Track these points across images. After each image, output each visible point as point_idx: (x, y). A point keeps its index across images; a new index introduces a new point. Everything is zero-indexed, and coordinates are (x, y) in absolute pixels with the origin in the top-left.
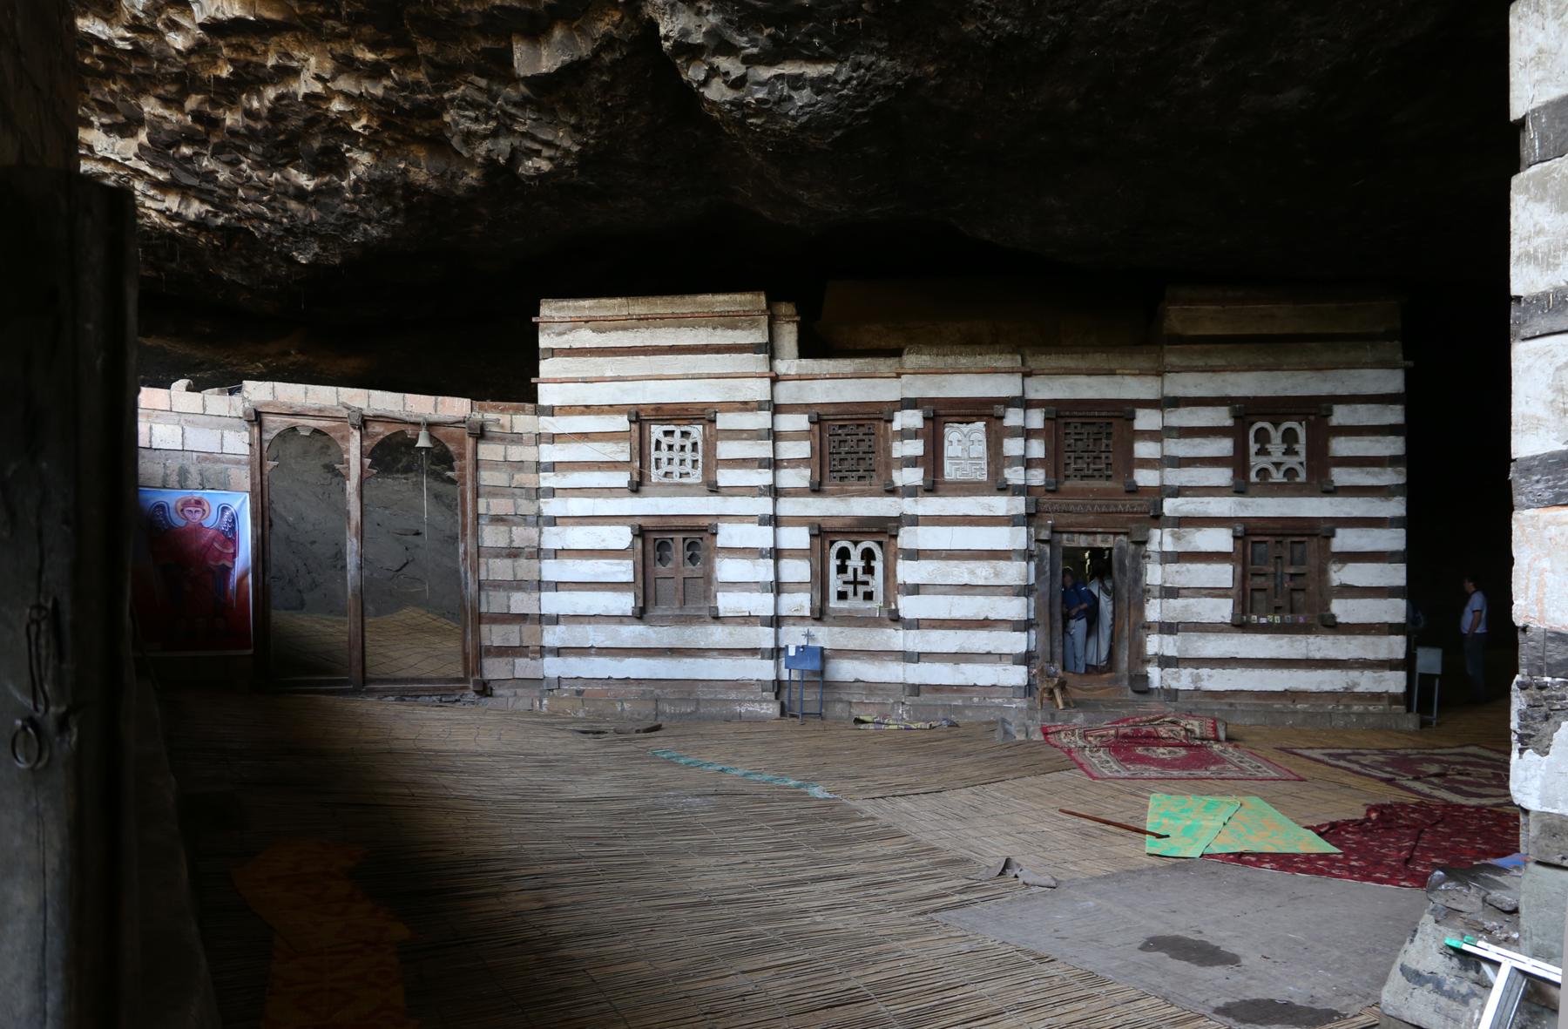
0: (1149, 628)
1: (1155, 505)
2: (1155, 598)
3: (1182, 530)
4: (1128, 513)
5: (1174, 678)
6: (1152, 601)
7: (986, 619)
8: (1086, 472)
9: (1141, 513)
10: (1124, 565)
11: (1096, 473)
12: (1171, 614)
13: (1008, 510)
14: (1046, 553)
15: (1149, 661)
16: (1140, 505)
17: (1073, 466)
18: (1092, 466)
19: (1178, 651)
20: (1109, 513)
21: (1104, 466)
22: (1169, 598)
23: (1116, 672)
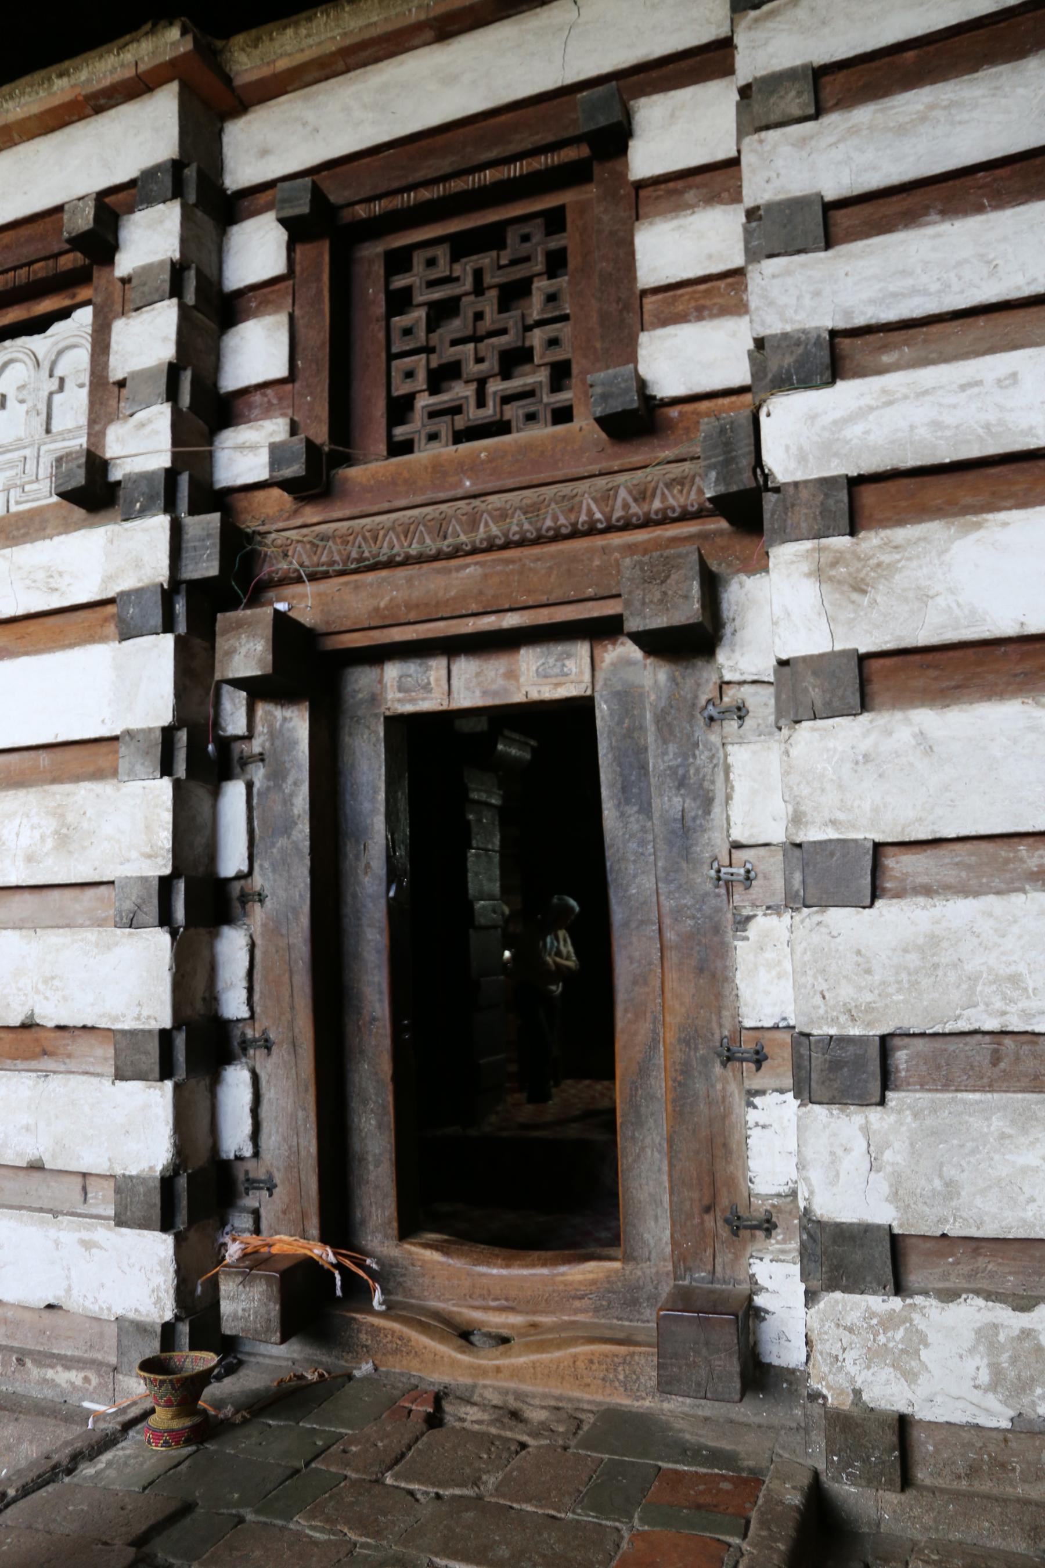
3: (871, 540)
4: (627, 526)
7: (28, 1026)
8: (474, 415)
9: (685, 516)
11: (513, 412)
12: (846, 993)
13: (108, 579)
14: (295, 743)
17: (424, 401)
18: (495, 387)
21: (542, 376)
23: (627, 1258)
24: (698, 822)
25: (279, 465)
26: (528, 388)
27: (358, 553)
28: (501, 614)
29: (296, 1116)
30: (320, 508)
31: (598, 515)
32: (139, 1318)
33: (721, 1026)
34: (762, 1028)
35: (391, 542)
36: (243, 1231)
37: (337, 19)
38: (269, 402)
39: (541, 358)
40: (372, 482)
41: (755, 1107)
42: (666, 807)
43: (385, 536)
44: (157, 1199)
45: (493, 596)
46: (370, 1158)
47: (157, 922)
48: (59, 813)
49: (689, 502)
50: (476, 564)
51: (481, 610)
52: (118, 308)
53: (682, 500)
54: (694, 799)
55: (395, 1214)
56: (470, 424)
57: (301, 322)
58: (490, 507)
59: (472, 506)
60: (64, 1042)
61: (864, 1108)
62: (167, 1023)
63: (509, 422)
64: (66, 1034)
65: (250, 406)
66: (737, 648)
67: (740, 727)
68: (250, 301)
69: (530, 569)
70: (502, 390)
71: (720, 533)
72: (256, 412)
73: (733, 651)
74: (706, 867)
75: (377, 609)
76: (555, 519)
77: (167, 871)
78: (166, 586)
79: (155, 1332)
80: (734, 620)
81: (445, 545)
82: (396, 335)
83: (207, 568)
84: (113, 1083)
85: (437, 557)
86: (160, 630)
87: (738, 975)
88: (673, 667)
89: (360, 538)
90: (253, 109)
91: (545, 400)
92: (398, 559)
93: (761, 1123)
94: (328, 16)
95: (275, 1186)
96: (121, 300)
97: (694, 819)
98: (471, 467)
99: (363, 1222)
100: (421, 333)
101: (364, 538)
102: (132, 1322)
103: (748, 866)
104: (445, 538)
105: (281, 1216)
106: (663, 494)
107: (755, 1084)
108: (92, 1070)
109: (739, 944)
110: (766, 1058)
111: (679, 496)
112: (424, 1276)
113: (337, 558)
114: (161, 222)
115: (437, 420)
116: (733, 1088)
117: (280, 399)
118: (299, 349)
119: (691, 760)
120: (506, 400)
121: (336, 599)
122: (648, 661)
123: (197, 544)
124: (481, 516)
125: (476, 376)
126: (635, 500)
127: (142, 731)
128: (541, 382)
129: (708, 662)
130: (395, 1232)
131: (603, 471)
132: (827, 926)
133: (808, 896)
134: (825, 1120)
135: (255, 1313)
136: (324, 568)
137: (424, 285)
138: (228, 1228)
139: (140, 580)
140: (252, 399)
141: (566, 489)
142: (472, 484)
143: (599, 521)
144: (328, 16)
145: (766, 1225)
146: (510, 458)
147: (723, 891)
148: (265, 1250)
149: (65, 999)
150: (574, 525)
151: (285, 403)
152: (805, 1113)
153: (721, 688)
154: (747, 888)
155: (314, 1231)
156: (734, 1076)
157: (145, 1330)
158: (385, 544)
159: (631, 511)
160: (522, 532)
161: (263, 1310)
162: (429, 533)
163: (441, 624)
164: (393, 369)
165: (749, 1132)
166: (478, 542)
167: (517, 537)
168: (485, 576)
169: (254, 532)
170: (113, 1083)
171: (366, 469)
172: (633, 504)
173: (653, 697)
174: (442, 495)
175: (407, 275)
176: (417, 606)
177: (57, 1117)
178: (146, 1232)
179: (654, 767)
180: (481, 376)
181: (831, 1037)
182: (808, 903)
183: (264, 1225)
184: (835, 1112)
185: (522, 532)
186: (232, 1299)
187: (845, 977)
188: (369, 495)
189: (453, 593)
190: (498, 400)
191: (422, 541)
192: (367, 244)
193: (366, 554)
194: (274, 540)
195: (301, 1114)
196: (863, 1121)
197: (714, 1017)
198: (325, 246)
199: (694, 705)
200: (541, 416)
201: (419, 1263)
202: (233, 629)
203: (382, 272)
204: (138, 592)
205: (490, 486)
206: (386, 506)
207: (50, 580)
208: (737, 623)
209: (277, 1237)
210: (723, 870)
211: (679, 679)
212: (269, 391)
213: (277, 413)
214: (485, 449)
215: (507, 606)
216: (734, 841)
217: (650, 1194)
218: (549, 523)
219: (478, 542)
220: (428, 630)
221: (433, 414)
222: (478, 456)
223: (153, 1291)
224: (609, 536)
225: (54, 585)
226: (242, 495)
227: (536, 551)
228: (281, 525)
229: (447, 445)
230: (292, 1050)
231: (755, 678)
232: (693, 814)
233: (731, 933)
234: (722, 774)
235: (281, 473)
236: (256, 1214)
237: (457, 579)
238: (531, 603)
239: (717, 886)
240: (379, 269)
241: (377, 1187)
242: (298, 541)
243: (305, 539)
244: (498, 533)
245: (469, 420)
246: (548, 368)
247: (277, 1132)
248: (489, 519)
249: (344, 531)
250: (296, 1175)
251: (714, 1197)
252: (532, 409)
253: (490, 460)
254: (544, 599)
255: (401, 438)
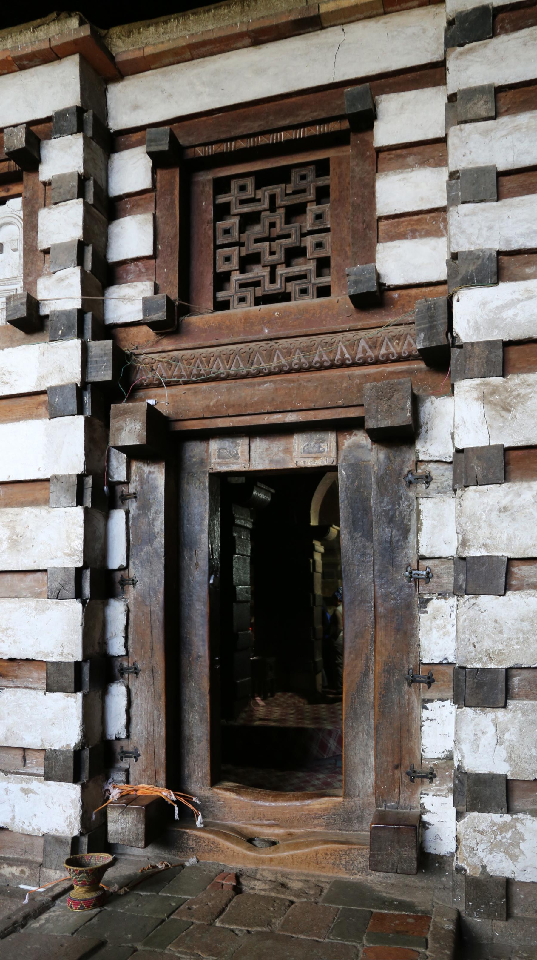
0: (430, 681)
1: (432, 318)
2: (443, 595)
4: (364, 363)
5: (494, 847)
6: (436, 604)
9: (400, 359)
10: (367, 510)
13: (41, 378)
15: (431, 776)
16: (398, 338)
17: (236, 277)
19: (509, 759)
20: (310, 369)
22: (477, 594)
24: (400, 543)
25: (149, 312)
26: (302, 273)
27: (197, 370)
28: (285, 414)
29: (153, 714)
30: (172, 341)
31: (347, 356)
32: (57, 834)
33: (408, 662)
34: (433, 664)
35: (218, 365)
36: (119, 782)
37: (185, 24)
38: (140, 270)
39: (311, 254)
40: (206, 326)
41: (427, 709)
42: (382, 534)
43: (214, 361)
44: (71, 764)
45: (281, 402)
46: (195, 739)
47: (74, 596)
48: (11, 526)
49: (403, 351)
50: (271, 381)
51: (273, 410)
52: (41, 201)
53: (399, 349)
54: (398, 530)
55: (209, 771)
56: (265, 293)
57: (160, 220)
58: (280, 346)
59: (269, 345)
60: (14, 669)
61: (495, 709)
62: (79, 658)
63: (290, 294)
64: (14, 664)
65: (127, 272)
66: (428, 441)
67: (427, 488)
68: (126, 204)
69: (304, 387)
70: (286, 273)
71: (419, 370)
72: (131, 276)
73: (426, 442)
74: (404, 570)
75: (208, 407)
76: (321, 356)
77: (80, 564)
78: (79, 385)
79: (68, 842)
80: (427, 423)
81: (253, 369)
82: (219, 233)
83: (104, 375)
84: (45, 694)
85: (247, 376)
86: (76, 413)
87: (421, 633)
88: (389, 450)
89: (198, 361)
90: (128, 77)
91: (313, 281)
92: (222, 376)
93: (430, 718)
94: (178, 21)
95: (139, 755)
96: (43, 196)
97: (398, 541)
98: (269, 321)
99: (189, 776)
100: (236, 233)
101: (201, 362)
102: (53, 837)
103: (428, 570)
104: (252, 364)
105: (142, 773)
106: (387, 345)
107: (427, 696)
108: (30, 685)
109: (422, 615)
110: (434, 681)
111: (396, 346)
112: (225, 807)
113: (184, 373)
114: (70, 147)
115: (245, 289)
116: (414, 698)
117: (147, 269)
118: (160, 237)
119: (397, 507)
120: (289, 279)
121: (182, 398)
122: (374, 446)
123: (98, 359)
124: (275, 352)
125: (270, 263)
126: (370, 348)
127: (65, 476)
128: (310, 270)
129: (410, 448)
130: (209, 782)
131: (351, 329)
132: (478, 606)
133: (468, 588)
134: (472, 716)
135: (130, 830)
136: (176, 379)
137: (238, 202)
138: (110, 781)
139: (62, 380)
140: (129, 267)
141: (328, 338)
142: (269, 332)
143: (348, 359)
144: (178, 21)
145: (430, 776)
146: (293, 316)
147: (413, 584)
148: (134, 793)
149: (15, 642)
150: (332, 361)
151: (150, 272)
152: (461, 712)
153: (416, 464)
154: (427, 583)
155: (163, 782)
156: (415, 691)
157: (61, 842)
158: (215, 366)
159: (367, 354)
160: (300, 363)
161: (134, 829)
162: (242, 361)
163: (248, 418)
164: (217, 255)
165: (423, 723)
166: (272, 368)
167: (296, 367)
168: (276, 390)
169: (132, 353)
170: (45, 694)
171: (203, 318)
172: (369, 350)
173: (376, 468)
174: (251, 338)
175: (227, 195)
176: (234, 406)
177: (9, 714)
178: (63, 783)
179: (375, 510)
180: (273, 263)
181: (478, 669)
182: (469, 592)
183: (132, 778)
184: (478, 712)
185: (300, 363)
186: (115, 822)
187: (487, 635)
188: (204, 335)
189: (256, 399)
190: (283, 279)
191: (238, 366)
192: (202, 173)
193: (202, 372)
194: (143, 360)
195: (156, 713)
196: (494, 717)
197: (405, 657)
198: (176, 172)
199: (400, 474)
200: (310, 291)
201: (223, 800)
202: (121, 415)
203: (211, 192)
204: (62, 388)
205: (281, 334)
206: (215, 342)
207: (3, 376)
208: (429, 426)
209: (141, 785)
210: (414, 572)
211: (392, 458)
212: (140, 264)
213: (145, 278)
214: (278, 310)
215: (289, 409)
216: (421, 555)
217: (361, 759)
218: (317, 359)
219: (272, 368)
220: (240, 421)
221: (242, 286)
222: (274, 314)
223: (67, 818)
224: (353, 368)
225: (6, 380)
226: (123, 329)
227: (308, 375)
228: (148, 350)
229: (251, 306)
230: (151, 675)
231: (438, 459)
232: (397, 538)
233: (417, 609)
234: (415, 515)
235: (151, 317)
236: (127, 771)
237: (259, 390)
238: (304, 408)
239: (410, 582)
240: (209, 190)
241: (198, 756)
242: (159, 361)
243: (164, 360)
244: (286, 364)
245: (265, 291)
246: (315, 261)
247: (141, 723)
248: (280, 354)
249: (188, 356)
250: (152, 749)
251: (401, 760)
252: (305, 286)
253: (280, 317)
254: (312, 406)
255: (222, 299)
